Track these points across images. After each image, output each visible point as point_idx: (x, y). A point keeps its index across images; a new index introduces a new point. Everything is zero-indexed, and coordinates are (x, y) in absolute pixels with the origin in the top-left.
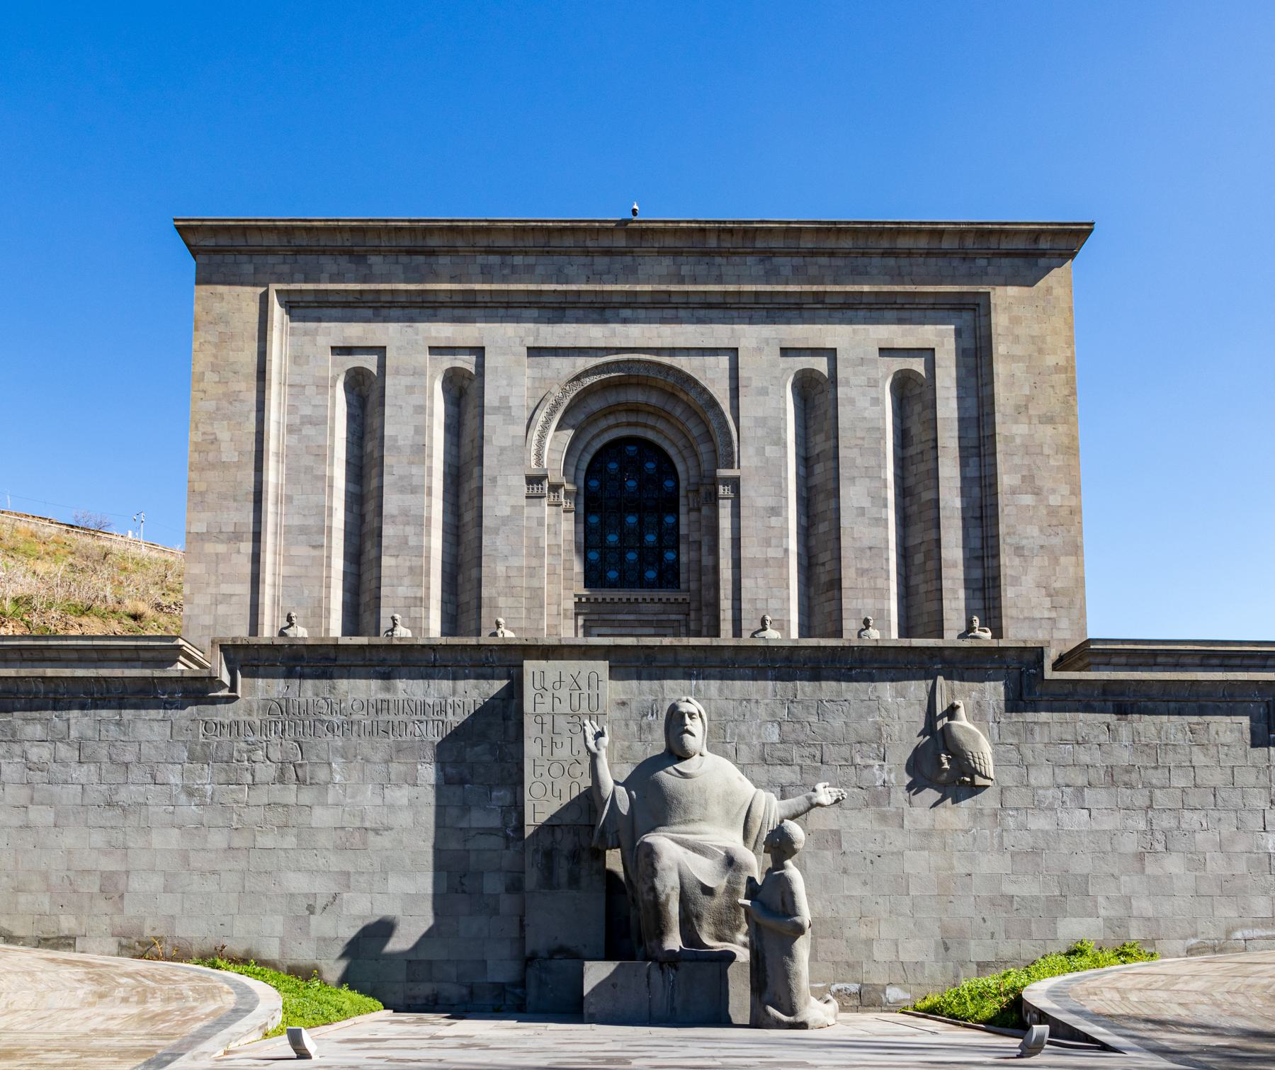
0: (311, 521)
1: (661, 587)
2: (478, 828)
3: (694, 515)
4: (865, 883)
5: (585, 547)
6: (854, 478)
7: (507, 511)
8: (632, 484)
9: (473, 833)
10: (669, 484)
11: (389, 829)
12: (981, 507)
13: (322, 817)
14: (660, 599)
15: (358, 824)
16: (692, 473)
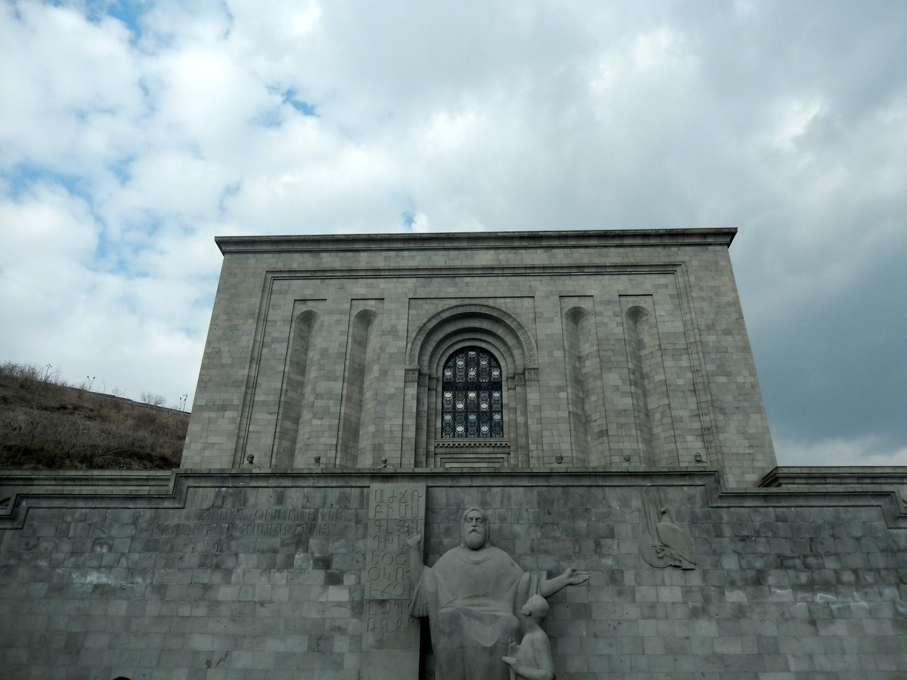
0: (271, 398)
1: (491, 436)
2: (332, 602)
3: (511, 392)
4: (611, 645)
5: (442, 412)
6: (611, 368)
7: (392, 391)
8: (472, 373)
10: (496, 373)
11: (271, 602)
12: (694, 384)
13: (226, 593)
14: (490, 444)
15: (250, 598)
16: (511, 366)
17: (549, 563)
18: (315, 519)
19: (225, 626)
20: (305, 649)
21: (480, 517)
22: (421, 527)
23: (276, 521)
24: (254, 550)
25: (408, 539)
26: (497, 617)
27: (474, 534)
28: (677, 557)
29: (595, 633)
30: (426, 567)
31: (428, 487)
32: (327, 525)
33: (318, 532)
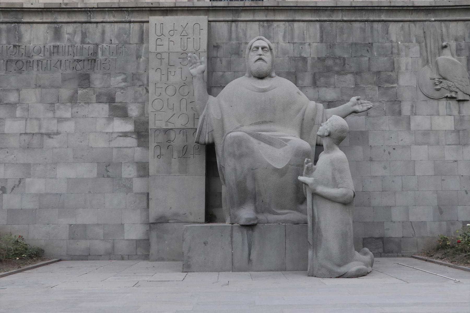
4: (385, 168)
9: (115, 135)
11: (58, 133)
15: (36, 130)
17: (330, 94)
18: (95, 53)
19: (15, 157)
20: (95, 175)
21: (267, 46)
22: (204, 58)
23: (55, 58)
24: (36, 85)
25: (192, 69)
26: (287, 141)
27: (260, 62)
28: (454, 89)
29: (370, 157)
30: (211, 97)
31: (209, 21)
32: (107, 60)
33: (99, 67)
